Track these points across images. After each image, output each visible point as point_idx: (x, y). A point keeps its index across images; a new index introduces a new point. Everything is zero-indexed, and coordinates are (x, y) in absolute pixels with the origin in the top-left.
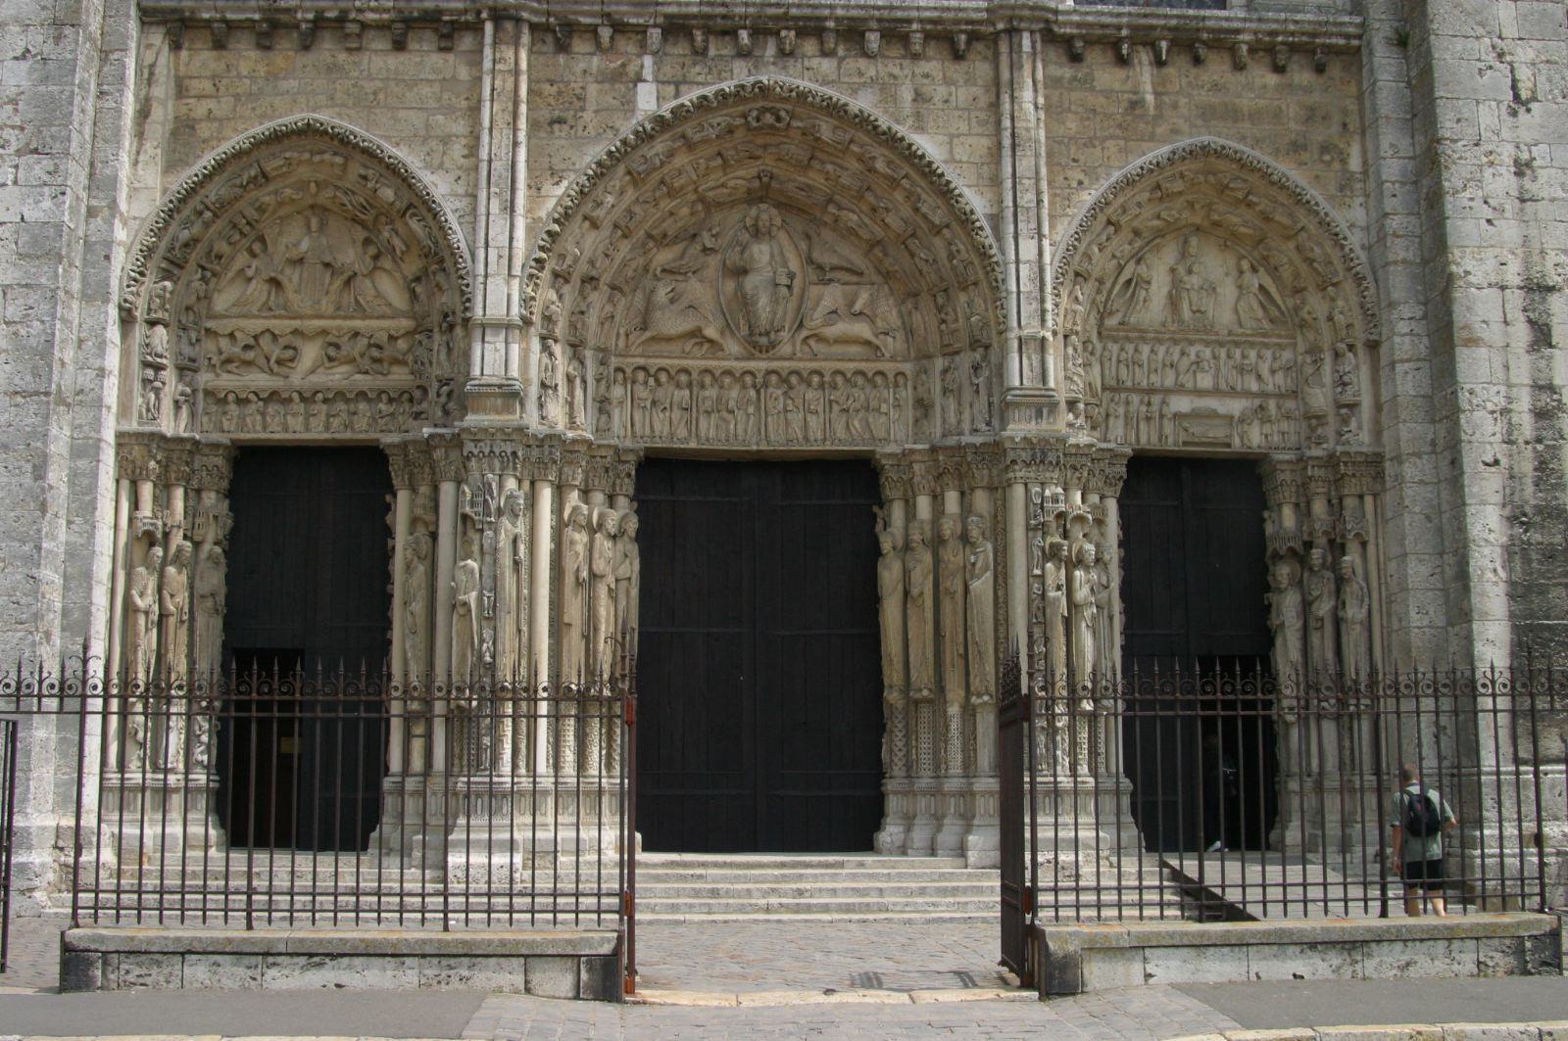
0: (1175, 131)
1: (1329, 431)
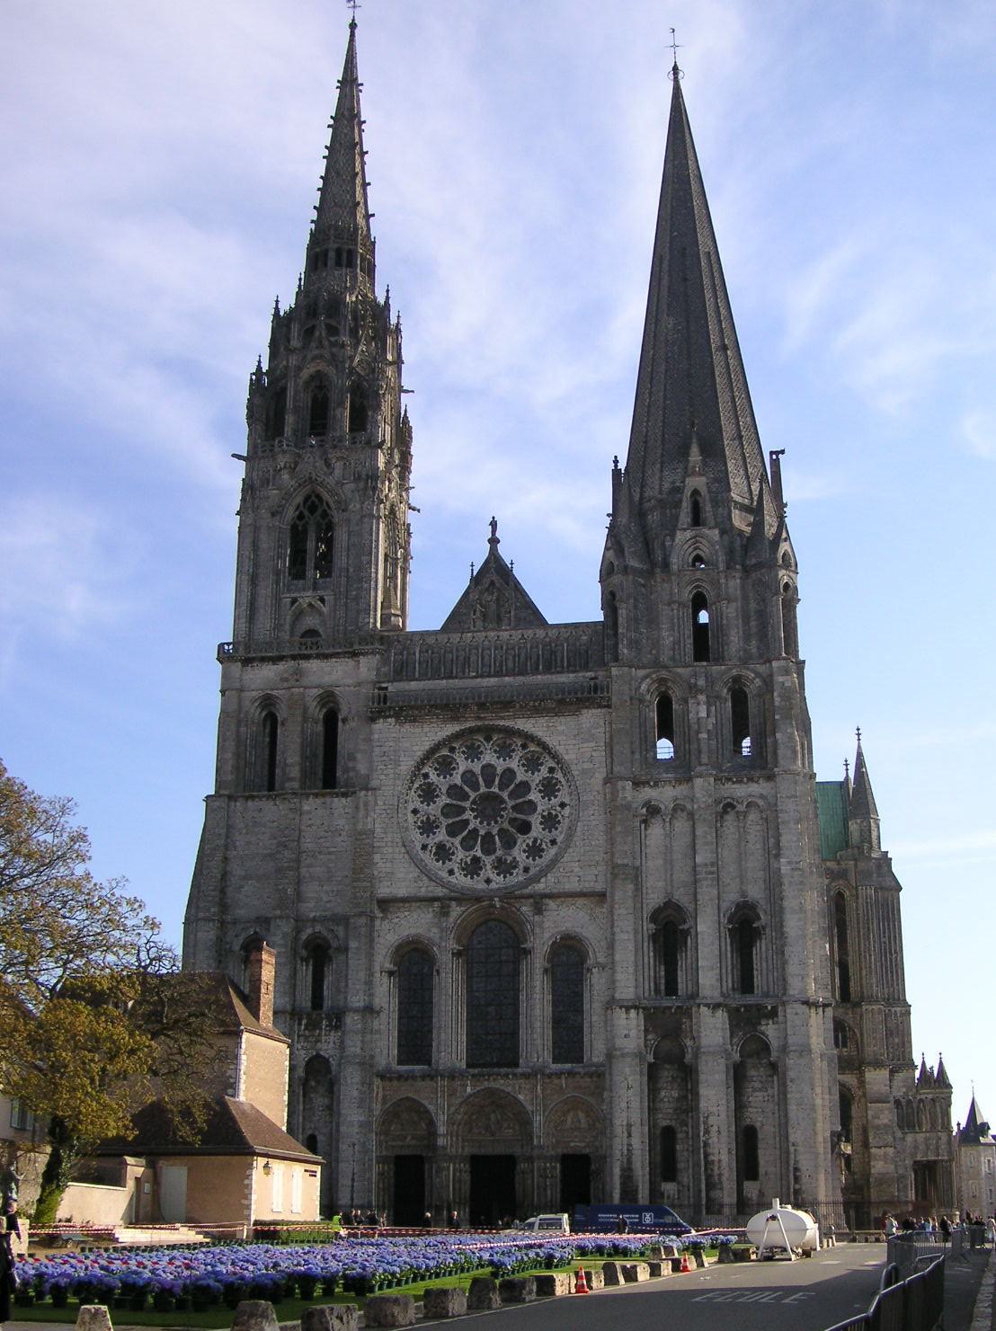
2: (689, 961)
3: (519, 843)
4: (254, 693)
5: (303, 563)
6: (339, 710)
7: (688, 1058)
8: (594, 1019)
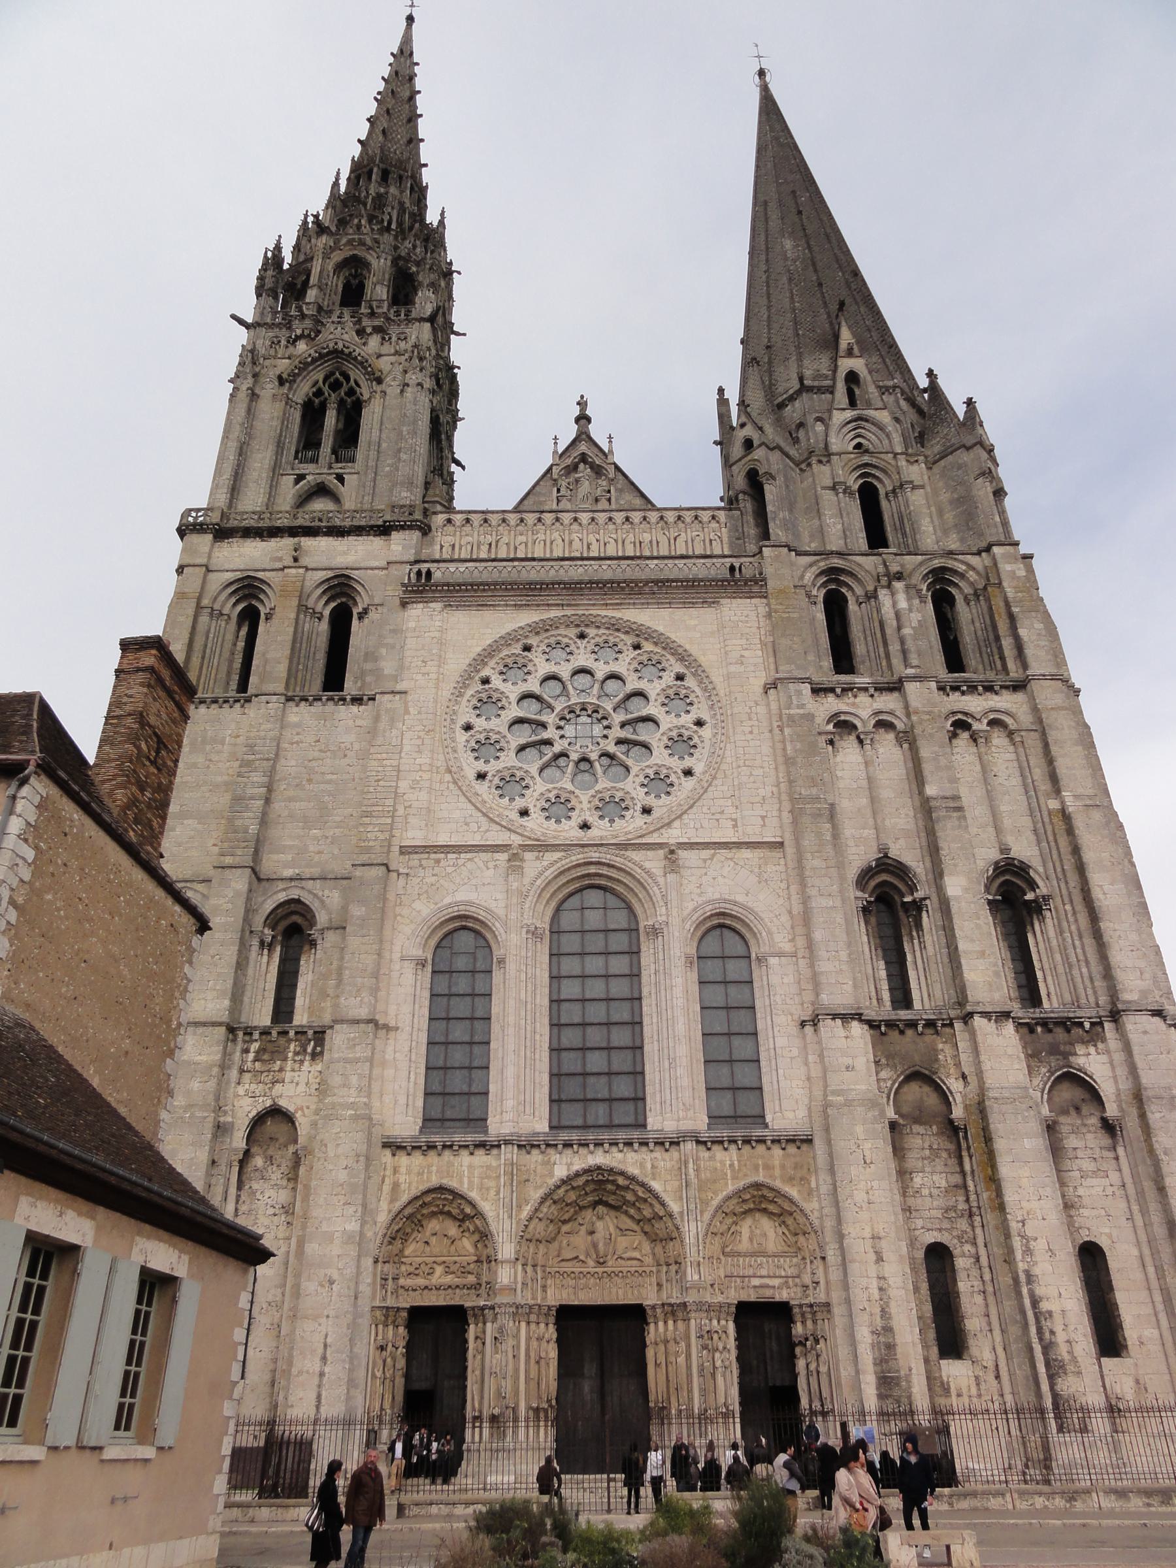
0: (745, 1175)
1: (810, 1292)
2: (930, 950)
3: (633, 771)
4: (230, 576)
5: (317, 445)
6: (356, 603)
7: (958, 1112)
8: (781, 1042)
